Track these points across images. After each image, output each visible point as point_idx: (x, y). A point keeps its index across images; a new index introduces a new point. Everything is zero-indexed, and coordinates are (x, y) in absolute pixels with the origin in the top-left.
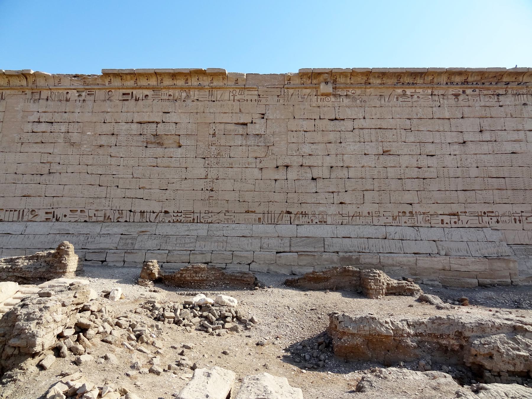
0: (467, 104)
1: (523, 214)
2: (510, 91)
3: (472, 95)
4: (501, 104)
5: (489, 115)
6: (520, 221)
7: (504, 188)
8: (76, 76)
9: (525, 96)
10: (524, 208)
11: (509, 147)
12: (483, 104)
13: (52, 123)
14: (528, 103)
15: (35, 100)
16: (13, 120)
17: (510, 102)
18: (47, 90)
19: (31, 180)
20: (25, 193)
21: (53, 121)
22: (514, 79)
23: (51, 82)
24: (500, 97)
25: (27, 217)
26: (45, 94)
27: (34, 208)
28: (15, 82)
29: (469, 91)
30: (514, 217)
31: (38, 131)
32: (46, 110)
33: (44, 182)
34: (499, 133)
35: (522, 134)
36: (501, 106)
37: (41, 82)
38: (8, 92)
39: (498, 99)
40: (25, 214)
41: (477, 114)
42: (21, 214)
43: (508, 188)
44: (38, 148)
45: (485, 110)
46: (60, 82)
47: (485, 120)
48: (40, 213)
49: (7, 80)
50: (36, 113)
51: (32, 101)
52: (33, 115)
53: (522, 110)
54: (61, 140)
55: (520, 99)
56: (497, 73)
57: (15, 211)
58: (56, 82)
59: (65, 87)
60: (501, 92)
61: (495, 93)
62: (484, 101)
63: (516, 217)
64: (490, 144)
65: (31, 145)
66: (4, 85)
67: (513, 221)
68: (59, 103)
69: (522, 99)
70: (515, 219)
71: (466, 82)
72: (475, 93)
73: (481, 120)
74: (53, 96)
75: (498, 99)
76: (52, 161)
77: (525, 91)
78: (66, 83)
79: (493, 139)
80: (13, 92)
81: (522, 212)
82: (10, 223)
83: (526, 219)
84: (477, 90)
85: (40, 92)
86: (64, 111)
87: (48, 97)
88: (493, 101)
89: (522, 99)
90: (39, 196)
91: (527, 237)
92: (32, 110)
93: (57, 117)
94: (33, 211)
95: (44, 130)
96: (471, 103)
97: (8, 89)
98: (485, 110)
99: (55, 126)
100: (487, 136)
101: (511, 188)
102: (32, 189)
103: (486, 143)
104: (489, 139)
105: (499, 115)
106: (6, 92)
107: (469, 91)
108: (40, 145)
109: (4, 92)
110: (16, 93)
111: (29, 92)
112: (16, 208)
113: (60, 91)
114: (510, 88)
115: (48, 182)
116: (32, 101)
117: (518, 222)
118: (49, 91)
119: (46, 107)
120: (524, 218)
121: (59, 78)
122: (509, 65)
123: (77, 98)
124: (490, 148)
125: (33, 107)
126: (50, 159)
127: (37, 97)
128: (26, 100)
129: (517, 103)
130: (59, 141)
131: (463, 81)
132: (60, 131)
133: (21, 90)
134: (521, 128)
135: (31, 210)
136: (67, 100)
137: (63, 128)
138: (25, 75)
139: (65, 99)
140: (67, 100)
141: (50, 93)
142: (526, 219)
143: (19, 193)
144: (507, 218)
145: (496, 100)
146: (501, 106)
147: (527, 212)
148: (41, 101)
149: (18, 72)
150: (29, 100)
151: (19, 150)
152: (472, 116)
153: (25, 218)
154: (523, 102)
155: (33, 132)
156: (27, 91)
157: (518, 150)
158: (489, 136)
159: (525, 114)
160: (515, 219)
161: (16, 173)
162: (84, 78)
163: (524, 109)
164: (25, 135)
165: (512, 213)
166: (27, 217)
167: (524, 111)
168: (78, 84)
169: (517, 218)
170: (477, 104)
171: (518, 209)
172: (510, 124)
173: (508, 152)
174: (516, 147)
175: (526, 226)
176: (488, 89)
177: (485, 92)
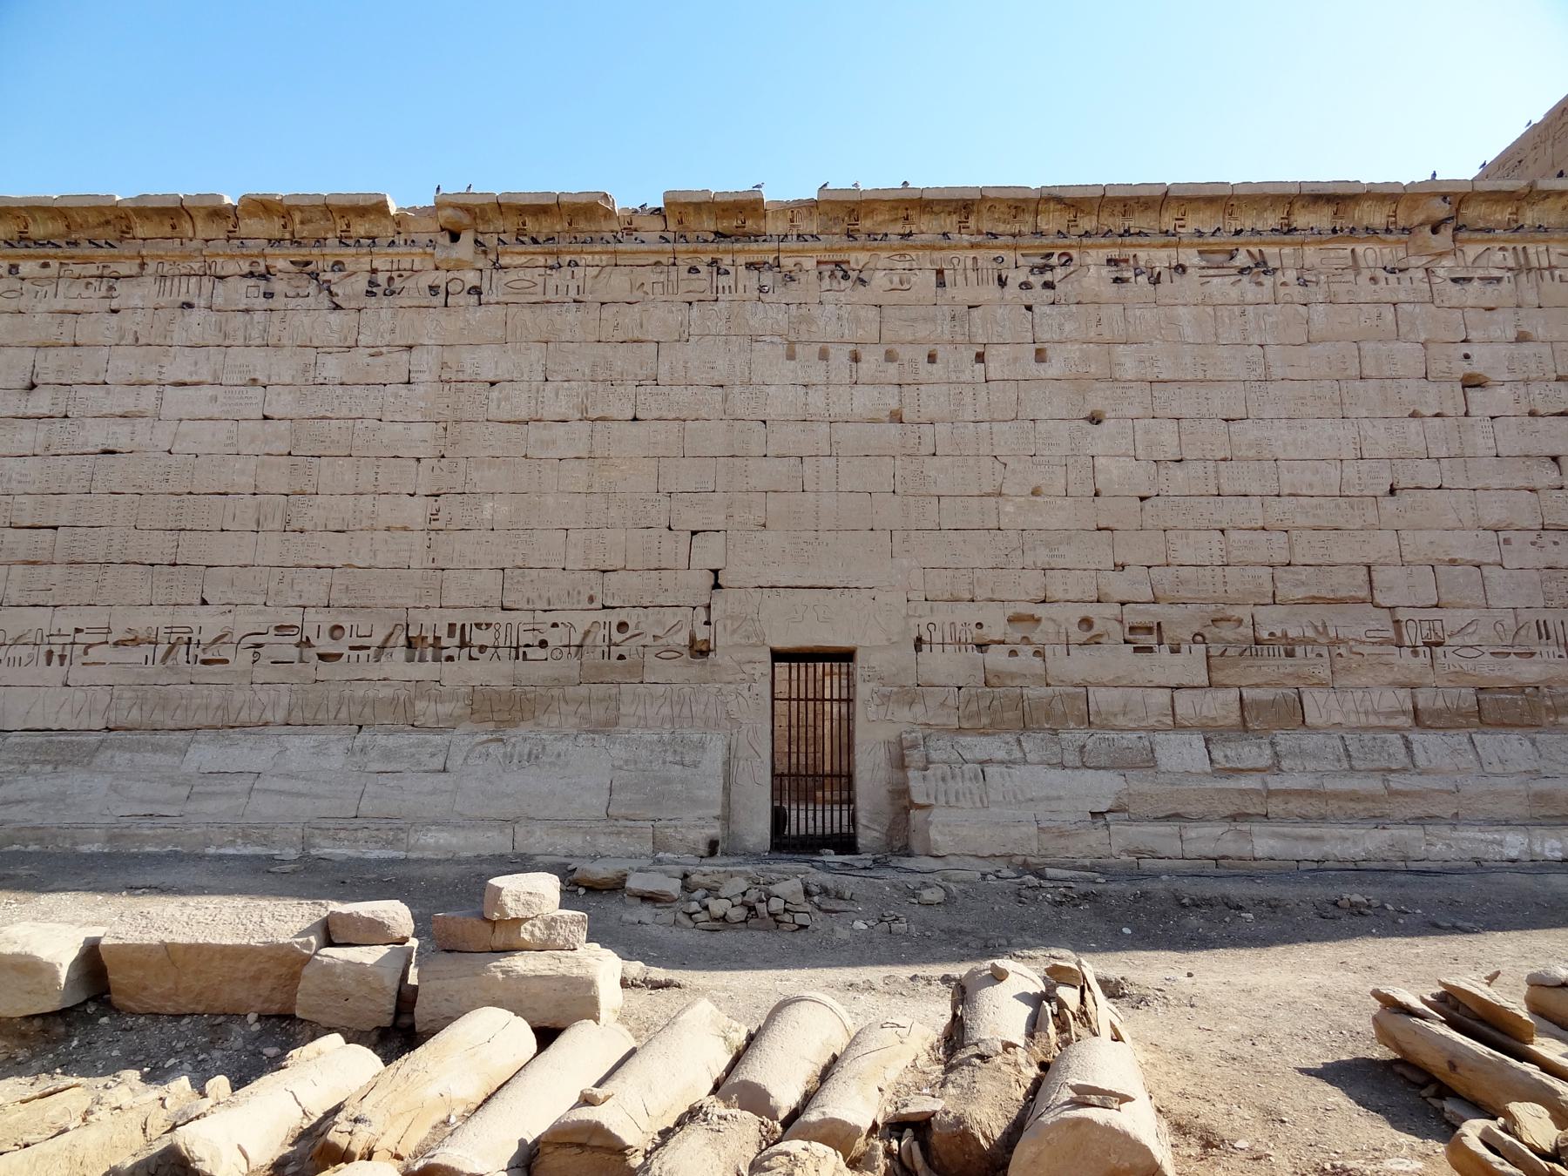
0: (13, 305)
1: (80, 638)
2: (151, 267)
3: (35, 280)
4: (115, 304)
5: (66, 340)
6: (62, 657)
7: (46, 557)
9: (193, 280)
10: (87, 618)
11: (98, 436)
12: (59, 305)
14: (195, 301)
17: (143, 298)
22: (168, 229)
24: (117, 285)
29: (27, 268)
30: (47, 648)
34: (83, 391)
35: (148, 396)
36: (115, 311)
39: (111, 288)
41: (34, 337)
43: (58, 557)
45: (61, 324)
47: (52, 352)
53: (171, 322)
55: (175, 290)
56: (99, 210)
60: (124, 268)
61: (106, 272)
62: (69, 296)
63: (54, 648)
64: (44, 426)
67: (43, 659)
69: (184, 289)
70: (50, 653)
71: (24, 239)
72: (47, 272)
73: (41, 353)
75: (111, 288)
77: (196, 266)
79: (59, 410)
81: (78, 630)
83: (86, 653)
84: (54, 264)
88: (93, 298)
89: (184, 289)
91: (67, 708)
96: (23, 303)
98: (61, 324)
100: (41, 402)
101: (67, 559)
103: (32, 423)
104: (45, 411)
105: (101, 339)
107: (27, 268)
114: (153, 257)
117: (56, 659)
120: (78, 649)
122: (123, 191)
124: (41, 436)
129: (163, 301)
131: (16, 236)
134: (150, 377)
142: (86, 653)
144: (22, 652)
145: (103, 292)
146: (115, 311)
147: (93, 631)
152: (16, 342)
154: (183, 298)
157: (122, 443)
158: (49, 402)
159: (176, 336)
160: (50, 653)
163: (179, 320)
165: (46, 633)
167: (176, 327)
169: (57, 650)
170: (41, 307)
171: (65, 622)
172: (126, 363)
173: (92, 450)
174: (119, 435)
175: (78, 674)
176: (87, 260)
177: (77, 270)
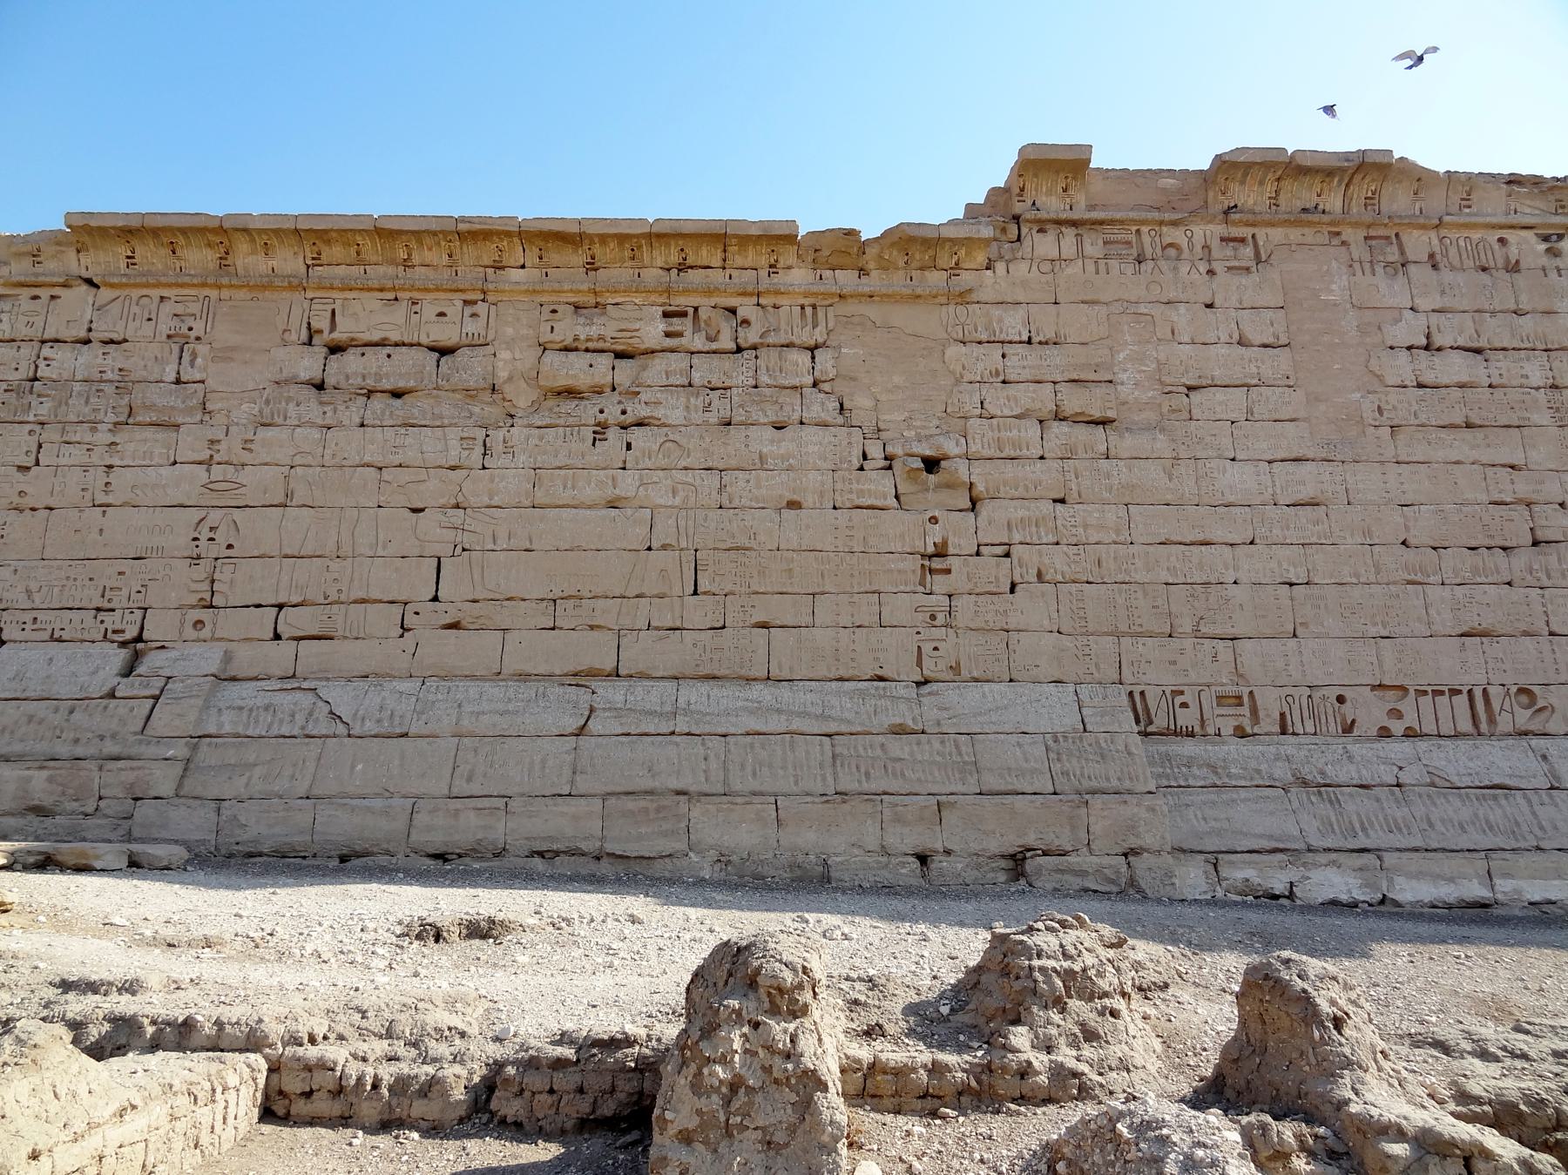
8: (1514, 180)
13: (1478, 351)
15: (1388, 264)
16: (1326, 338)
18: (1423, 227)
19: (1475, 571)
20: (1471, 621)
21: (1483, 343)
23: (1435, 203)
25: (1506, 716)
26: (1418, 243)
27: (1523, 681)
28: (1300, 195)
31: (1445, 380)
32: (1447, 302)
33: (1529, 577)
37: (1397, 200)
38: (1277, 234)
40: (1496, 706)
42: (1479, 703)
44: (1461, 446)
46: (1466, 202)
48: (1554, 701)
49: (1270, 189)
50: (1408, 314)
51: (1379, 269)
52: (1397, 321)
54: (1542, 417)
57: (1455, 692)
58: (1455, 199)
59: (1502, 220)
65: (1434, 434)
66: (1257, 209)
68: (1484, 277)
74: (1453, 251)
76: (1534, 497)
78: (1493, 206)
80: (1294, 234)
82: (1448, 742)
85: (1397, 235)
86: (1513, 307)
87: (1432, 256)
90: (1526, 634)
92: (1391, 302)
93: (1496, 331)
94: (1521, 691)
95: (1465, 378)
97: (1272, 224)
99: (1502, 367)
102: (1490, 604)
106: (1270, 237)
108: (1467, 434)
109: (1261, 233)
110: (1309, 239)
111: (1352, 235)
112: (1455, 683)
113: (1476, 235)
115: (1544, 577)
116: (1379, 269)
118: (1433, 234)
119: (1443, 292)
121: (1465, 185)
123: (1545, 261)
125: (1392, 292)
126: (1523, 488)
127: (1393, 254)
128: (1357, 266)
130: (1536, 418)
132: (1523, 381)
133: (1326, 229)
135: (1514, 689)
136: (1514, 268)
137: (1536, 371)
138: (1370, 169)
139: (1501, 263)
140: (1514, 268)
141: (1435, 241)
143: (1444, 620)
148: (1412, 268)
149: (1347, 156)
150: (1367, 266)
151: (1389, 453)
153: (1504, 723)
155: (1420, 386)
156: (1348, 233)
161: (1403, 543)
162: (1552, 188)
164: (1394, 396)
166: (1506, 716)
168: (1531, 210)
